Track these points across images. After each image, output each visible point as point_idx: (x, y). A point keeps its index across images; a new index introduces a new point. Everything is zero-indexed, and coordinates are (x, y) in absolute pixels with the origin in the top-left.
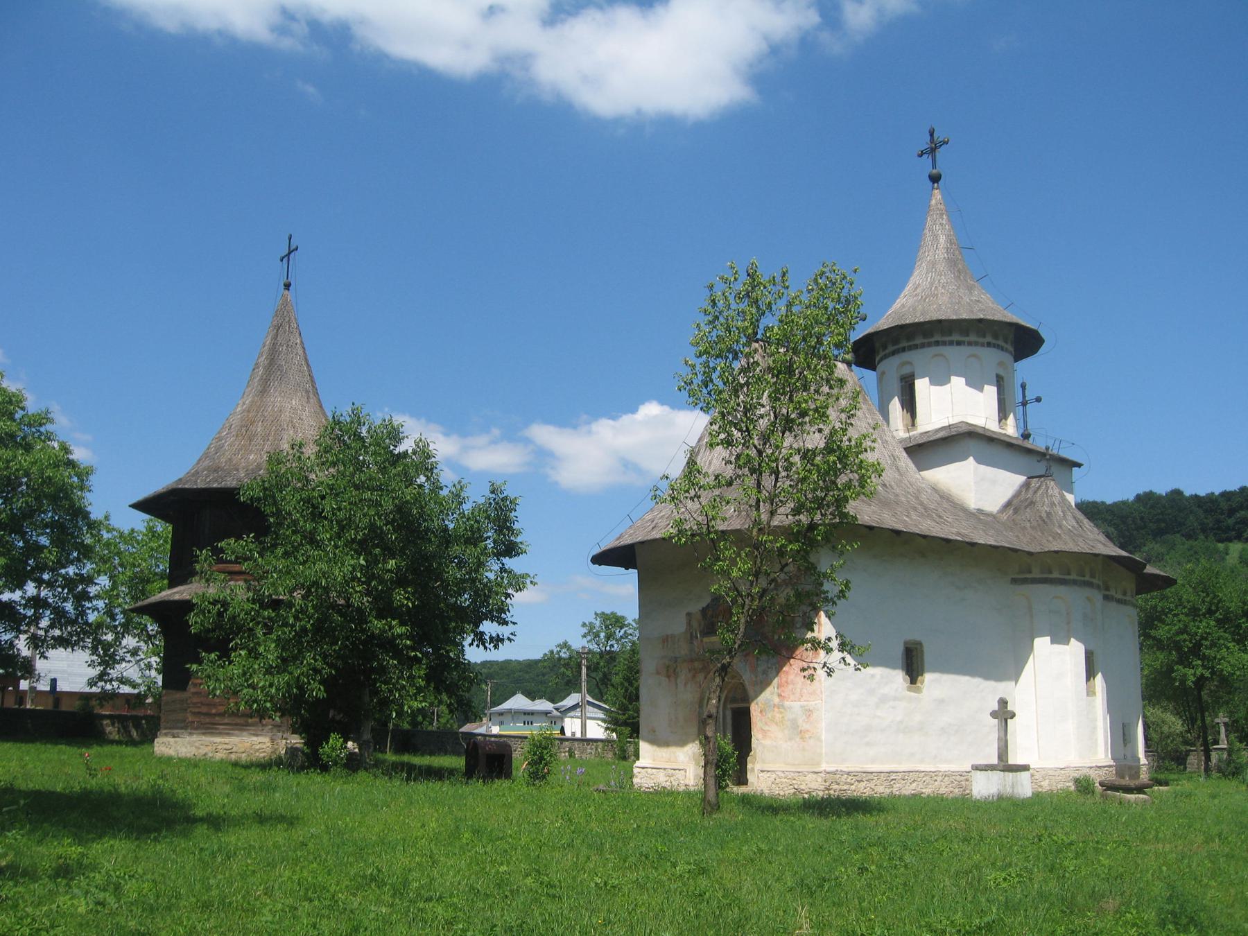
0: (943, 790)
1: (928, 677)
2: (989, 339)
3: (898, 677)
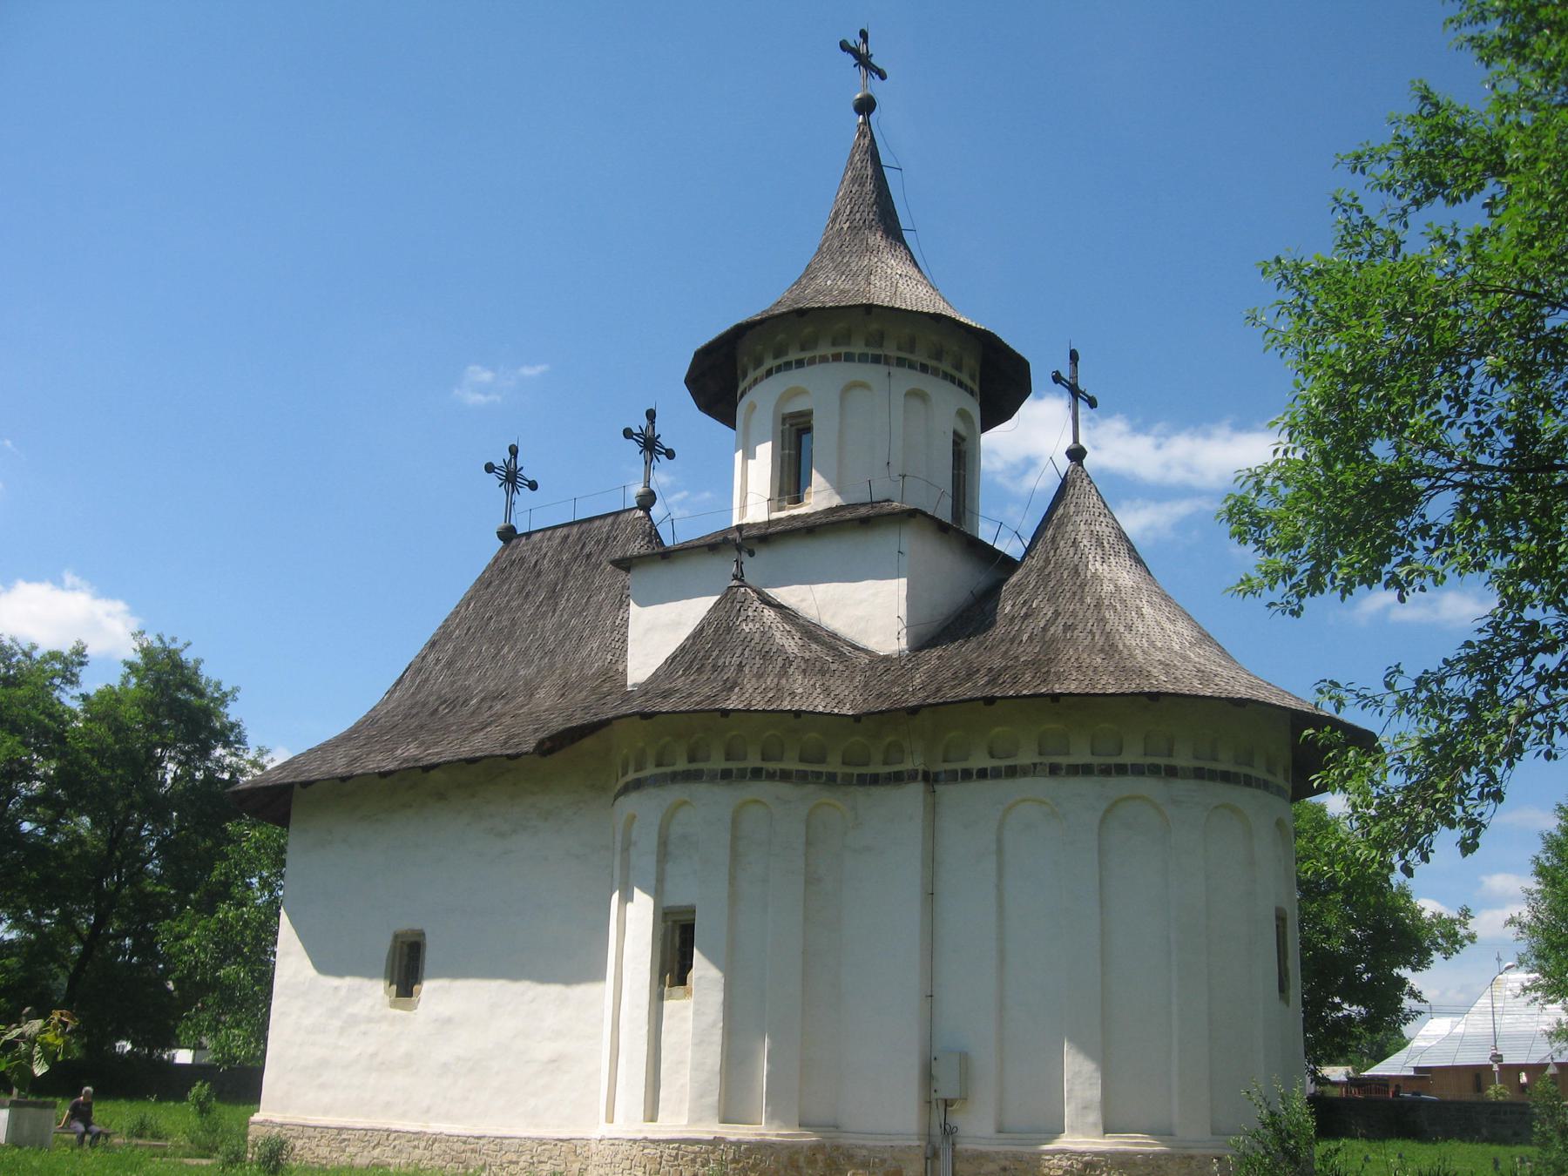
1: (428, 988)
2: (769, 363)
3: (377, 991)
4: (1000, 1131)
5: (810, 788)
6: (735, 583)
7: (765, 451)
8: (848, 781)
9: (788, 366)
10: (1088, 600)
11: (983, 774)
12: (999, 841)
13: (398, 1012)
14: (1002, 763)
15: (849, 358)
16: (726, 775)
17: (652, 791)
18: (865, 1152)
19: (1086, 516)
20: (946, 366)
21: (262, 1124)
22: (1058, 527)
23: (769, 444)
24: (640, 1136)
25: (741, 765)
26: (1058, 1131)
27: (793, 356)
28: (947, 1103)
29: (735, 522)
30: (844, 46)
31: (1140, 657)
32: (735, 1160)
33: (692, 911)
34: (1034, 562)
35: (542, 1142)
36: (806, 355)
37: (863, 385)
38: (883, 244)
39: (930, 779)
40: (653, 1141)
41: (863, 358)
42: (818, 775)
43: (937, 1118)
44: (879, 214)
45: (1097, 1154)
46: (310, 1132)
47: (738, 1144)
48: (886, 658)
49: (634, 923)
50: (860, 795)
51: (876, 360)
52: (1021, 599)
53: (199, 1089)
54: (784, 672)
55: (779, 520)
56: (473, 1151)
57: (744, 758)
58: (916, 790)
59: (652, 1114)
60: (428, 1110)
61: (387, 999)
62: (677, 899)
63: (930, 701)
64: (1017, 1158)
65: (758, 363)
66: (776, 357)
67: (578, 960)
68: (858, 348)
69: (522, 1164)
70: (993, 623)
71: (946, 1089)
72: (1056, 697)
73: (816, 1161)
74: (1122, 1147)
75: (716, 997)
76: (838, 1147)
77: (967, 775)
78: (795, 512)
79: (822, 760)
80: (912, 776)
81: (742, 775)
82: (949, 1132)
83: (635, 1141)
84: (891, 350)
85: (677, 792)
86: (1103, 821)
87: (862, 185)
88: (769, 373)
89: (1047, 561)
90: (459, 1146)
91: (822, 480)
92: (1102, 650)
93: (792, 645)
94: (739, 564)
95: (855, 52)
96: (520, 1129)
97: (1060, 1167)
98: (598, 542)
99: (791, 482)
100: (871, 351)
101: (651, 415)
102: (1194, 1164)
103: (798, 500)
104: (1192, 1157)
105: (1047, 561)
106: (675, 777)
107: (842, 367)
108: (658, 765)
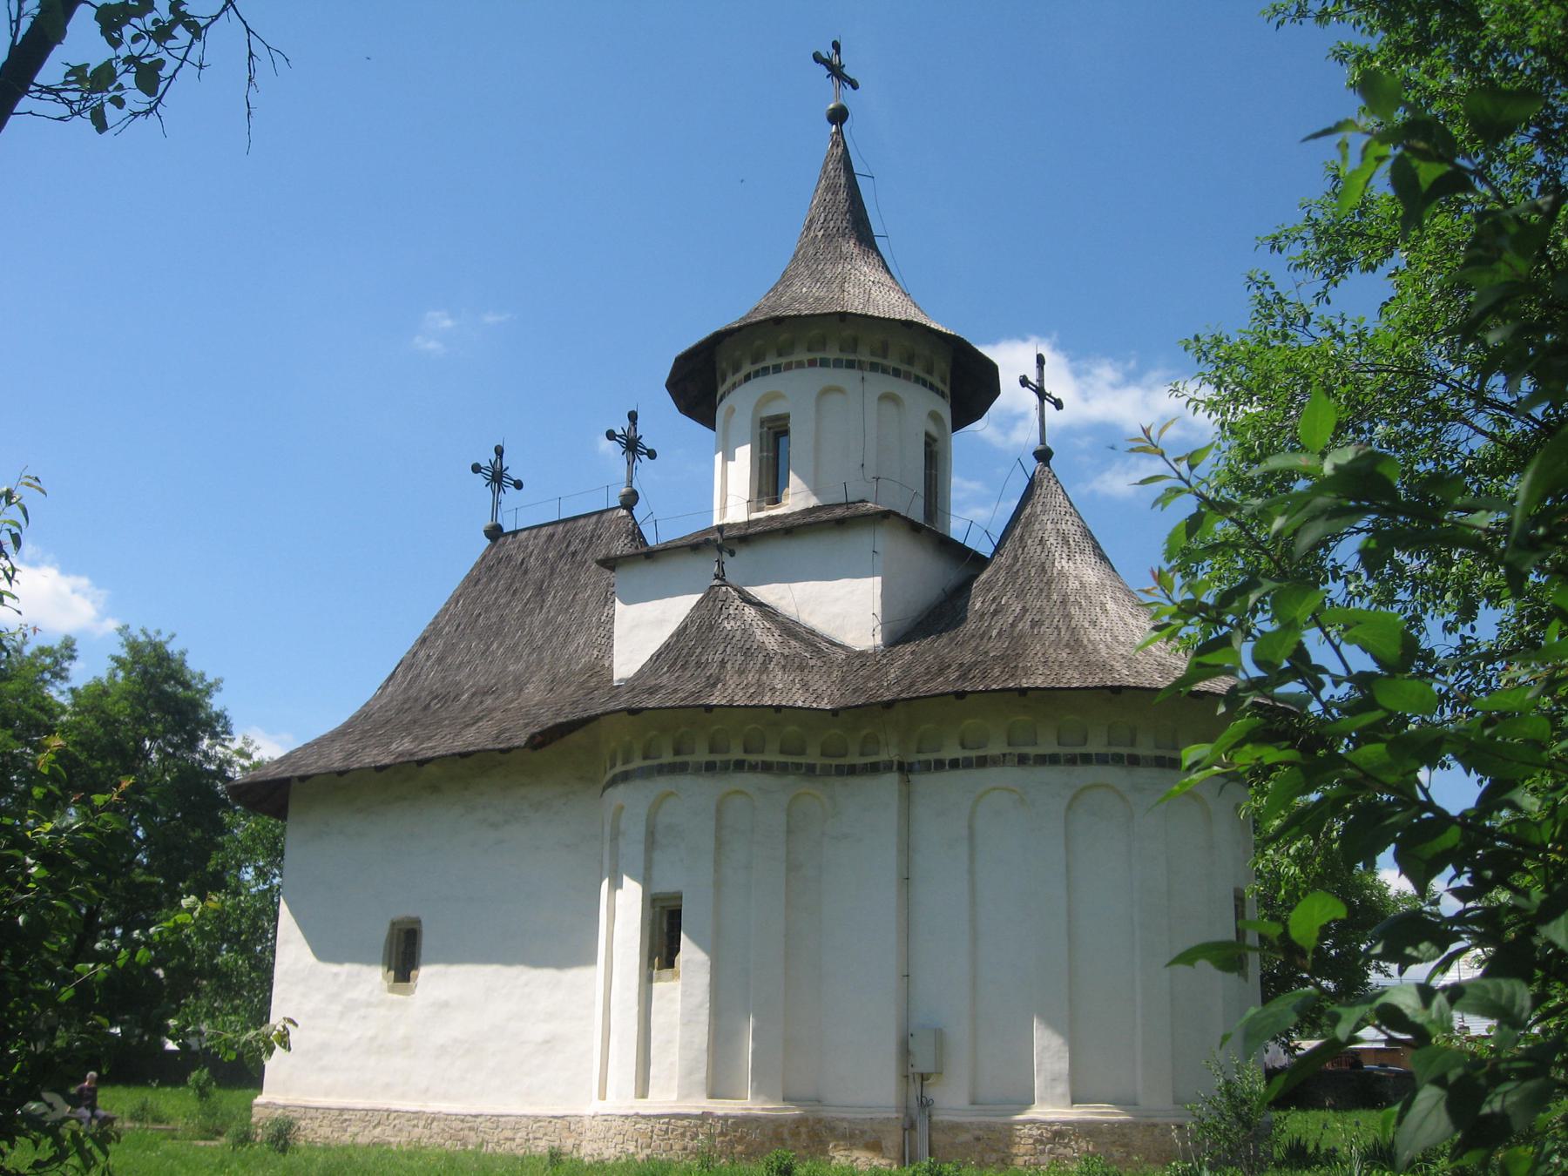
0: (424, 1141)
1: (425, 974)
2: (748, 368)
3: (376, 976)
4: (973, 1103)
5: (790, 779)
6: (716, 582)
7: (744, 453)
8: (827, 772)
9: (765, 371)
10: (1055, 597)
11: (955, 764)
12: (970, 827)
13: (395, 996)
14: (973, 754)
15: (824, 363)
16: (710, 767)
17: (638, 783)
18: (845, 1125)
19: (1052, 515)
20: (917, 370)
21: (266, 1106)
22: (1026, 525)
23: (748, 448)
24: (632, 1112)
25: (724, 757)
26: (1028, 1102)
27: (770, 361)
28: (924, 1077)
29: (717, 522)
30: (817, 58)
31: (1104, 651)
32: (722, 1134)
33: (678, 897)
34: (1003, 560)
35: (536, 1119)
36: (783, 361)
37: (839, 390)
38: (856, 251)
39: (905, 769)
40: (644, 1117)
41: (838, 364)
42: (798, 766)
43: (914, 1090)
44: (852, 221)
45: (1065, 1123)
46: (312, 1113)
47: (725, 1118)
48: (862, 654)
49: (623, 910)
50: (837, 783)
51: (851, 365)
52: (990, 596)
53: (198, 1075)
54: (764, 669)
55: (758, 521)
56: (471, 1129)
57: (728, 751)
58: (892, 780)
59: (643, 1091)
60: (427, 1090)
61: (385, 985)
62: (665, 886)
63: (904, 695)
64: (990, 1128)
65: (736, 370)
66: (753, 363)
67: (571, 945)
68: (832, 354)
69: (518, 1141)
70: (964, 619)
71: (923, 1063)
72: (1023, 692)
73: (799, 1134)
74: (1089, 1117)
75: (702, 980)
76: (820, 1121)
77: (939, 765)
78: (773, 512)
79: (802, 752)
80: (888, 767)
81: (726, 767)
82: (925, 1104)
83: (627, 1117)
84: (864, 356)
85: (663, 784)
86: (1069, 807)
87: (835, 193)
88: (747, 378)
89: (1016, 558)
90: (457, 1125)
91: (799, 481)
92: (1067, 645)
93: (772, 642)
94: (721, 564)
95: (827, 63)
96: (513, 1105)
97: (1031, 1136)
98: (583, 540)
99: (769, 483)
100: (845, 357)
101: (633, 417)
102: (1157, 1131)
103: (776, 501)
104: (1155, 1125)
105: (1016, 558)
106: (662, 770)
107: (817, 371)
108: (645, 758)
